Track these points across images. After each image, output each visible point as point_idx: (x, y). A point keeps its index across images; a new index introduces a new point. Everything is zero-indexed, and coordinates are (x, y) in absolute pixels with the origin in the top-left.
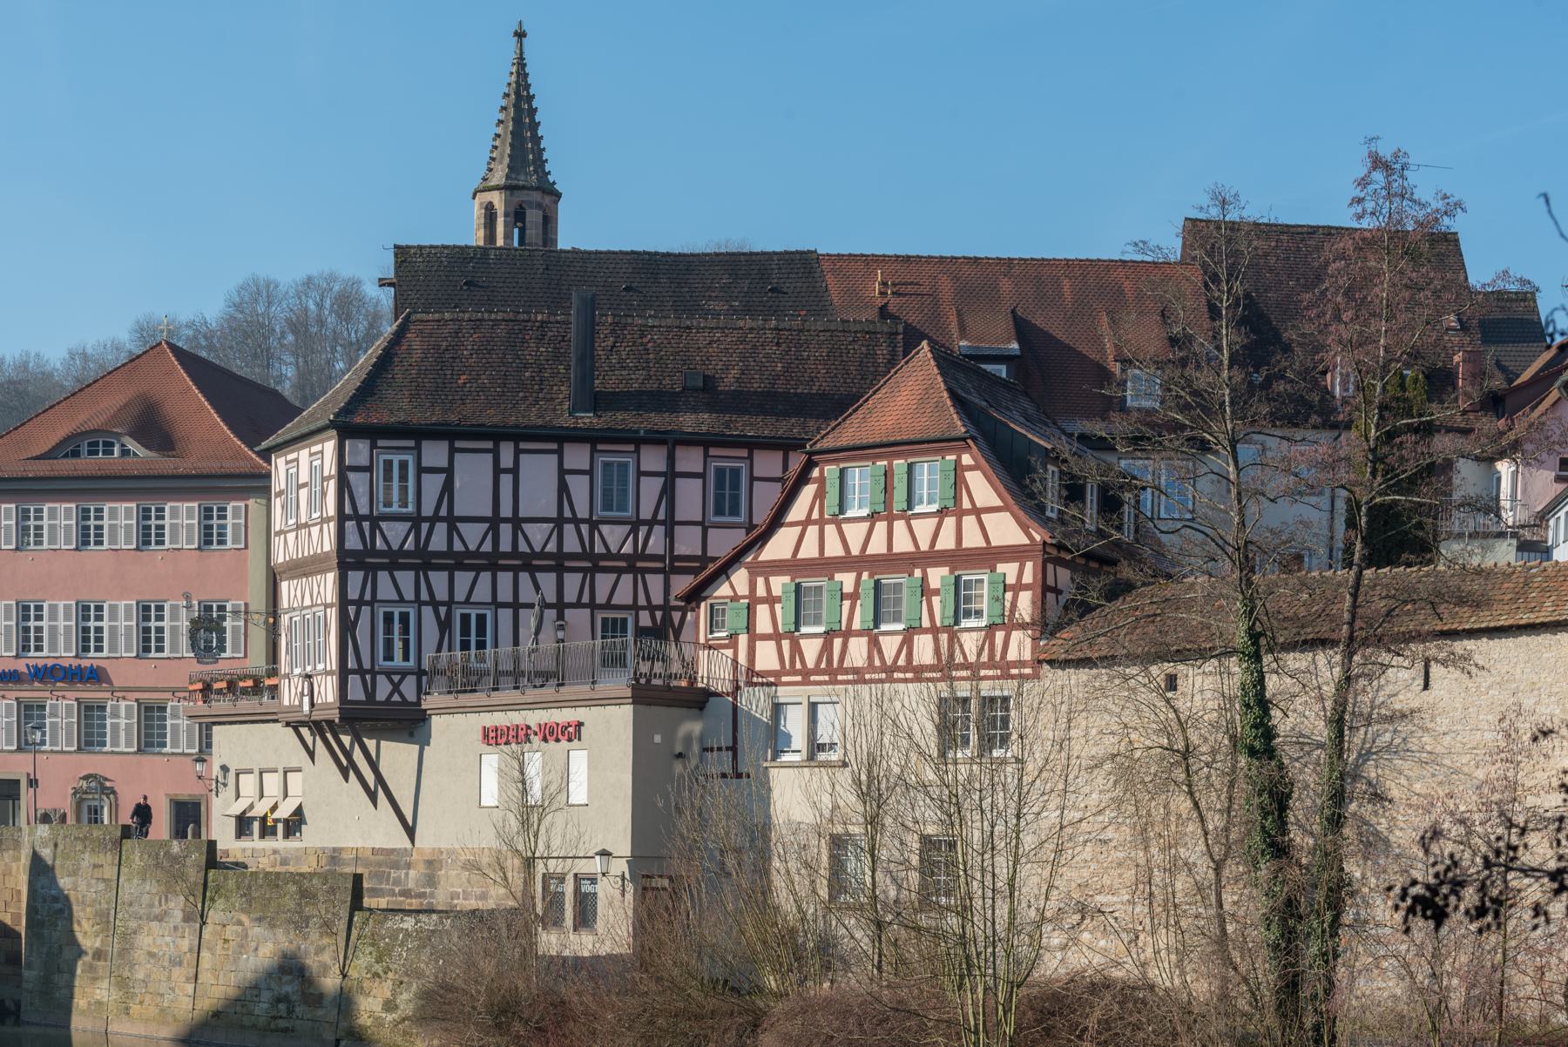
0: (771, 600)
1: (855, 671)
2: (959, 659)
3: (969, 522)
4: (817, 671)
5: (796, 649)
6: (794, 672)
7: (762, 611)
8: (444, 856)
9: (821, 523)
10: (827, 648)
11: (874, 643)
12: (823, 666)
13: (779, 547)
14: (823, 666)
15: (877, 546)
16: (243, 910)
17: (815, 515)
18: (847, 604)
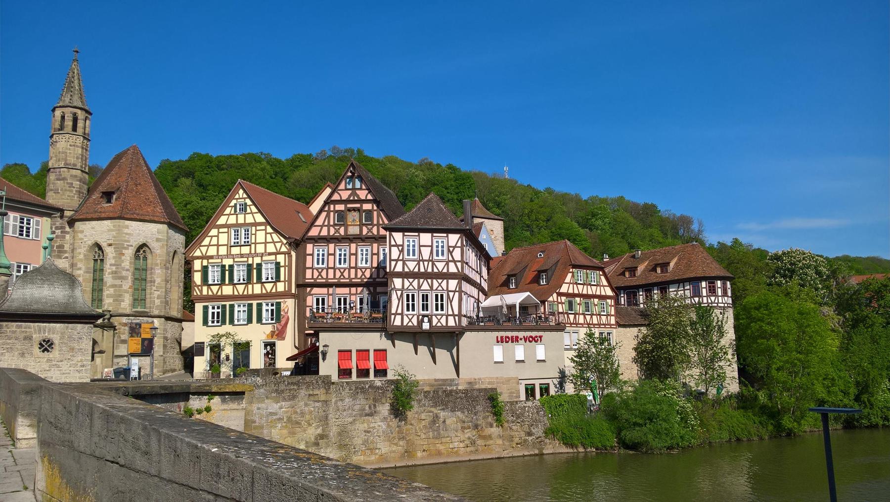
0: (562, 303)
2: (602, 323)
3: (602, 288)
5: (568, 317)
7: (560, 305)
9: (573, 284)
10: (575, 318)
11: (585, 318)
12: (575, 322)
13: (564, 289)
14: (575, 322)
15: (585, 292)
16: (432, 406)
17: (572, 282)
18: (578, 306)
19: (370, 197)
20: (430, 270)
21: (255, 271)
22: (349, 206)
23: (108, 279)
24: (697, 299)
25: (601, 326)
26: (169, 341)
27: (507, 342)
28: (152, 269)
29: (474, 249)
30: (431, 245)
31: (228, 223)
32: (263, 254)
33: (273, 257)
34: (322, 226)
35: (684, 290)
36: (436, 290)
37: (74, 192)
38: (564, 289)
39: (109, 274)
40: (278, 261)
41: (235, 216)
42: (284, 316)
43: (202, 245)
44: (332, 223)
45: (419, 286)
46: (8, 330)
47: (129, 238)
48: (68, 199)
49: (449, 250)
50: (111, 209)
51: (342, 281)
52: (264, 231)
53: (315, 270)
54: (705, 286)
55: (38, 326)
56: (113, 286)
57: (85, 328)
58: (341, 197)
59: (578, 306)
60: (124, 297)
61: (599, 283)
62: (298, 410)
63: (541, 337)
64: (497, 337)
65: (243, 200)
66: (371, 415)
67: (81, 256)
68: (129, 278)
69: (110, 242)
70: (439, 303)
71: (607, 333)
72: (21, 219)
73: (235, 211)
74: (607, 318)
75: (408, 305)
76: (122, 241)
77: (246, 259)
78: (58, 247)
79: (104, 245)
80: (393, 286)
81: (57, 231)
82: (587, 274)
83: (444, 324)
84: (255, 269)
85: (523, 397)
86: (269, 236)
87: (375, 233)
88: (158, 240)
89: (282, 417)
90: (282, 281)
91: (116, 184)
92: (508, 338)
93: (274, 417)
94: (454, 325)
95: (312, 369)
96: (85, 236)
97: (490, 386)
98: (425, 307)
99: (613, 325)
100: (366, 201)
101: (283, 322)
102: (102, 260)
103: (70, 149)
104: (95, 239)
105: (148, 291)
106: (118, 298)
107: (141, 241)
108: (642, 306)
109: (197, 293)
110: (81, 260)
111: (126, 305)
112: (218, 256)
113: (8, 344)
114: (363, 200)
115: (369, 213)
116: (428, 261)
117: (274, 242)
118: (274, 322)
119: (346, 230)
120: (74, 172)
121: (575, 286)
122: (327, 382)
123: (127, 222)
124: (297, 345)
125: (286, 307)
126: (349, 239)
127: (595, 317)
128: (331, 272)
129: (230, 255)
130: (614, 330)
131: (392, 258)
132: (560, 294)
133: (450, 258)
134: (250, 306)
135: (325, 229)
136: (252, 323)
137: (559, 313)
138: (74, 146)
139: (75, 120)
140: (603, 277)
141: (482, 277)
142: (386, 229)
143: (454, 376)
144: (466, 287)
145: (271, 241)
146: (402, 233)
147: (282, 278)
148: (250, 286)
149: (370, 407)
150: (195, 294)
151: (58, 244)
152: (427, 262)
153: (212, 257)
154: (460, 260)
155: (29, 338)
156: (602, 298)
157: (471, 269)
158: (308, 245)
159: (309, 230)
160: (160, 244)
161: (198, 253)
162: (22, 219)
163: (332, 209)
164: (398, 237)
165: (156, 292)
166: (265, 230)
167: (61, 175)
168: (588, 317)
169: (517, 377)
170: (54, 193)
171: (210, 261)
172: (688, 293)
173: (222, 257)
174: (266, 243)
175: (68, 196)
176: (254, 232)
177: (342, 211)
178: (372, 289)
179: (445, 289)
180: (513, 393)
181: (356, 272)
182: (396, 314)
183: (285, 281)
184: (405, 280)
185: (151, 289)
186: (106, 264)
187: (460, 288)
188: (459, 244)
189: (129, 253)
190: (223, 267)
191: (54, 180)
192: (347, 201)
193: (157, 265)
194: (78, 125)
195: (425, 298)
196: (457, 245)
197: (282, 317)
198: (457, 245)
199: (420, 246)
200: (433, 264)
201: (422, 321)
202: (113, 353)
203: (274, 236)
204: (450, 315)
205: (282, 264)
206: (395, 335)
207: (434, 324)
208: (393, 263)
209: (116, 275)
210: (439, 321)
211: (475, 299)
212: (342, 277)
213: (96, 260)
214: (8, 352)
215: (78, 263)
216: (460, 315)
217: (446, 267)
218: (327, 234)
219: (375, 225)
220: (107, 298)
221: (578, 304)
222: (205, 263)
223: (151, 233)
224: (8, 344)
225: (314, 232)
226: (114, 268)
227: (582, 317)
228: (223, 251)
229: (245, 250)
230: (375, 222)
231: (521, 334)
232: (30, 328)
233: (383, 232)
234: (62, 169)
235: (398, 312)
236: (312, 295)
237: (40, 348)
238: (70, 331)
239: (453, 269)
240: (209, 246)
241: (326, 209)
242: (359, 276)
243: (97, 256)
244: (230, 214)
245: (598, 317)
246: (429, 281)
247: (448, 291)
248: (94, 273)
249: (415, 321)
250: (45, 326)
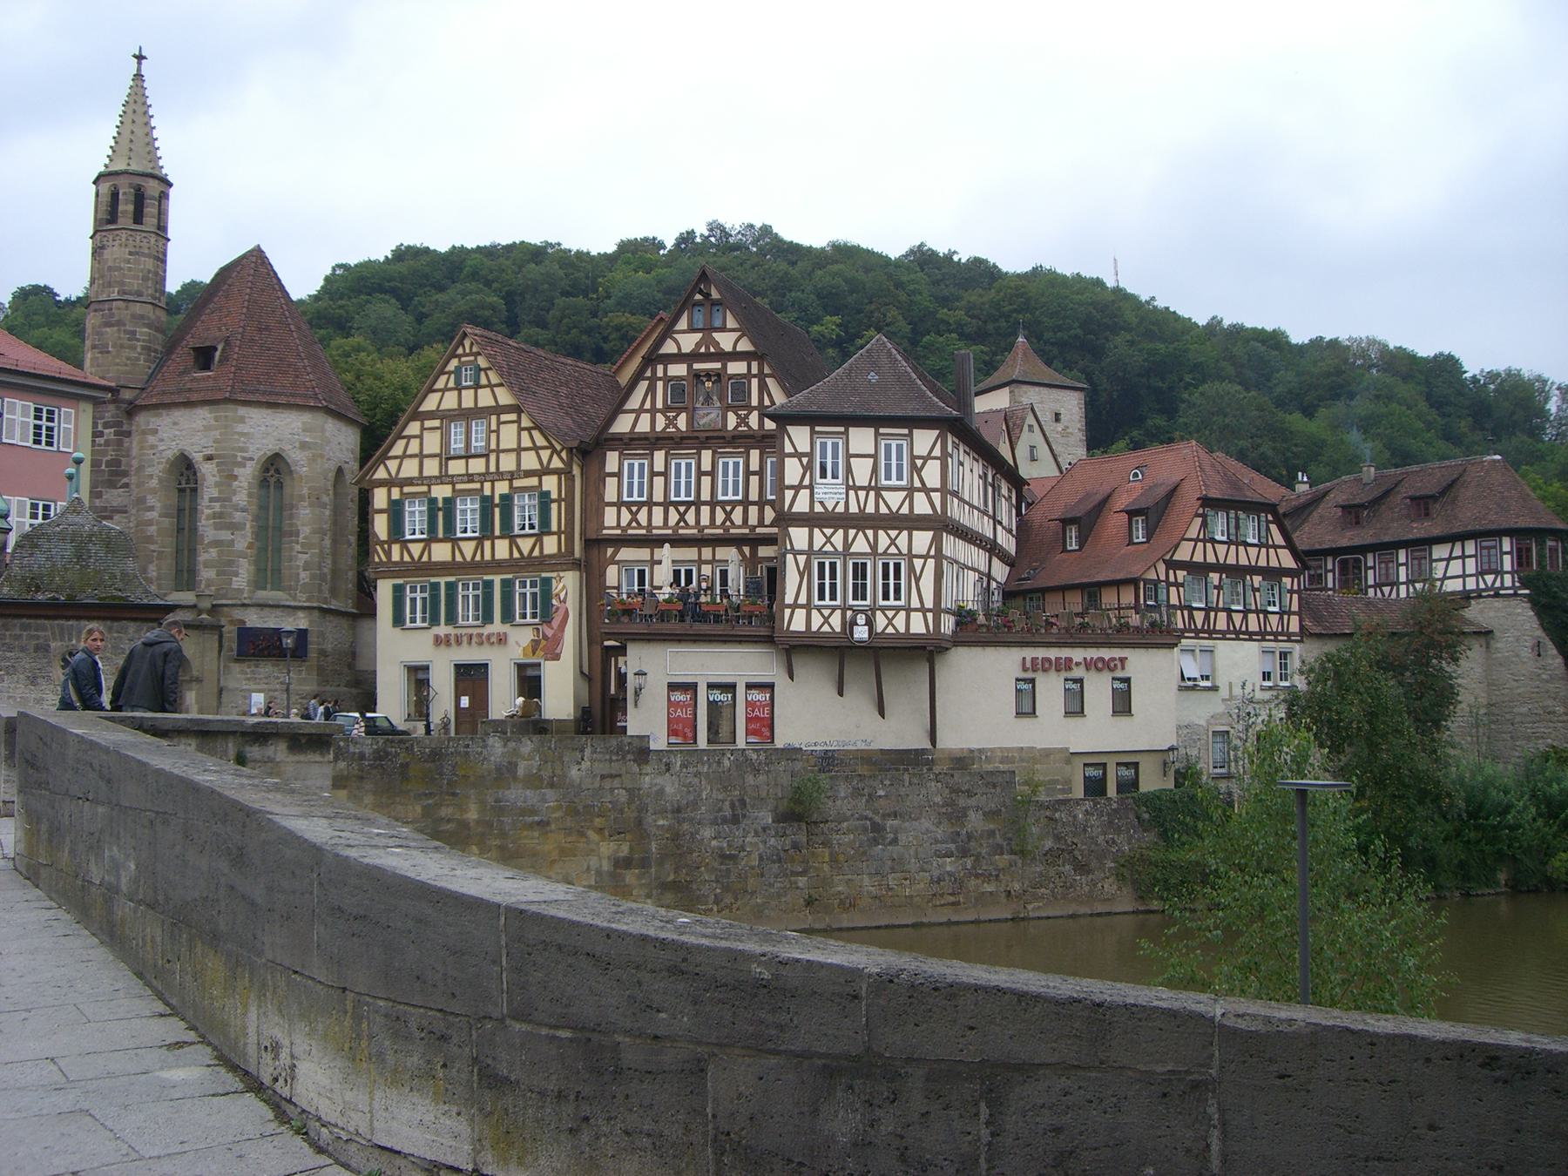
0: (1177, 585)
1: (1223, 633)
2: (1269, 629)
3: (1272, 551)
4: (1203, 631)
5: (1191, 617)
6: (1190, 631)
7: (1173, 590)
8: (976, 754)
9: (1204, 541)
10: (1207, 617)
11: (1230, 618)
15: (1231, 560)
17: (1201, 536)
18: (1216, 591)
19: (745, 346)
20: (870, 509)
21: (497, 510)
22: (696, 366)
23: (206, 529)
24: (1489, 578)
25: (1267, 637)
26: (329, 658)
27: (1045, 670)
28: (292, 507)
29: (977, 461)
30: (873, 452)
31: (441, 408)
32: (512, 473)
33: (534, 481)
34: (639, 412)
35: (1463, 557)
36: (885, 553)
37: (139, 350)
38: (1183, 554)
39: (208, 518)
40: (545, 488)
41: (456, 392)
42: (558, 609)
43: (391, 454)
44: (659, 405)
45: (847, 545)
46: (8, 633)
47: (244, 443)
48: (126, 365)
49: (913, 466)
50: (211, 383)
51: (681, 531)
52: (515, 426)
53: (624, 509)
54: (1509, 550)
55: (58, 625)
56: (216, 543)
57: (142, 629)
58: (679, 348)
59: (1216, 591)
60: (238, 567)
61: (1263, 540)
62: (580, 808)
63: (1123, 660)
64: (1024, 659)
65: (472, 358)
66: (735, 820)
67: (154, 483)
68: (248, 526)
69: (209, 452)
70: (892, 581)
71: (1281, 653)
72: (37, 410)
73: (458, 382)
74: (1281, 619)
75: (821, 588)
76: (233, 449)
77: (478, 486)
78: (109, 464)
79: (197, 457)
80: (789, 547)
81: (106, 431)
82: (1237, 519)
83: (902, 630)
84: (497, 506)
85: (1079, 792)
86: (525, 434)
87: (755, 427)
88: (304, 446)
89: (545, 819)
90: (554, 533)
91: (220, 330)
92: (1049, 660)
93: (530, 819)
94: (925, 631)
95: (619, 724)
96: (162, 440)
97: (1002, 767)
98: (860, 592)
99: (1294, 634)
100: (735, 356)
101: (555, 623)
102: (194, 490)
103: (129, 263)
104: (180, 447)
105: (285, 554)
107: (269, 446)
108: (1371, 592)
109: (379, 556)
110: (154, 491)
111: (242, 579)
112: (421, 479)
113: (9, 659)
114: (729, 353)
115: (741, 383)
116: (867, 489)
117: (536, 448)
118: (537, 620)
119: (690, 421)
120: (137, 309)
121: (1209, 545)
122: (642, 751)
123: (242, 411)
124: (586, 670)
125: (562, 590)
126: (697, 438)
127: (1252, 617)
128: (658, 512)
129: (447, 475)
130: (1297, 647)
131: (787, 482)
132: (1172, 565)
133: (917, 484)
134: (489, 585)
135: (645, 418)
136: (439, 625)
137: (1169, 606)
138: (137, 253)
139: (139, 199)
140: (1273, 527)
141: (1000, 523)
142: (772, 417)
143: (929, 746)
144: (951, 545)
145: (530, 445)
146: (808, 428)
147: (554, 528)
148: (487, 544)
149: (733, 806)
150: (377, 559)
151: (109, 458)
152: (865, 492)
153: (410, 481)
154: (939, 486)
155: (43, 649)
156: (1273, 574)
157: (967, 507)
158: (608, 453)
159: (611, 420)
160: (308, 453)
161: (381, 474)
162: (38, 410)
163: (660, 373)
164: (799, 437)
165: (300, 555)
166: (519, 421)
167: (112, 315)
168: (1237, 618)
169: (1067, 749)
170: (101, 353)
171: (406, 489)
172: (1471, 567)
173: (430, 481)
174: (519, 450)
175: (128, 359)
176: (494, 427)
177: (680, 378)
178: (747, 550)
179: (905, 551)
180: (1056, 782)
181: (713, 513)
182: (795, 606)
183: (559, 533)
184: (816, 530)
185: (292, 549)
186: (202, 498)
187: (939, 550)
188: (937, 452)
189: (247, 474)
190: (433, 501)
191: (99, 327)
192: (694, 357)
193: (302, 498)
194: (146, 210)
195: (860, 571)
196: (933, 454)
197: (554, 609)
198: (933, 454)
199: (849, 456)
200: (878, 496)
201: (854, 623)
202: (219, 680)
203: (536, 434)
204: (916, 610)
205: (554, 496)
206: (796, 649)
207: (879, 630)
208: (789, 494)
209: (222, 521)
210: (890, 622)
211: (979, 572)
212: (682, 524)
213: (181, 491)
214: (8, 674)
215: (149, 497)
216: (937, 610)
217: (907, 501)
218: (648, 430)
219: (755, 408)
220: (205, 567)
221: (1215, 587)
222: (396, 493)
223: (290, 431)
224: (9, 659)
225: (622, 425)
226: (217, 506)
227: (1222, 616)
228: (432, 468)
229: (477, 466)
230: (755, 402)
231: (1078, 655)
232: (44, 629)
233: (770, 425)
234: (114, 303)
235: (799, 602)
236: (618, 563)
237: (63, 668)
238: (115, 635)
239: (922, 506)
240: (404, 456)
241: (648, 374)
242: (719, 521)
243: (183, 482)
244: (443, 391)
245: (1261, 616)
246: (870, 533)
247: (911, 556)
248: (178, 516)
249: (836, 621)
250: (72, 625)
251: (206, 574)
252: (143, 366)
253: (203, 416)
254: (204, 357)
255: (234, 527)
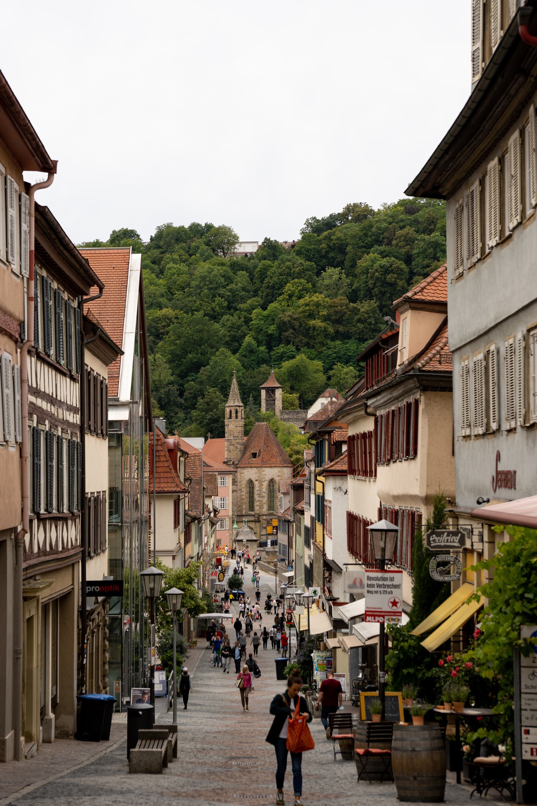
56: (259, 501)
79: (254, 480)
88: (279, 476)
106: (261, 507)
120: (237, 441)
123: (264, 469)
139: (237, 412)
189: (265, 484)
251: (256, 508)
252: (240, 455)
253: (254, 470)
254: (254, 455)
255: (263, 497)
